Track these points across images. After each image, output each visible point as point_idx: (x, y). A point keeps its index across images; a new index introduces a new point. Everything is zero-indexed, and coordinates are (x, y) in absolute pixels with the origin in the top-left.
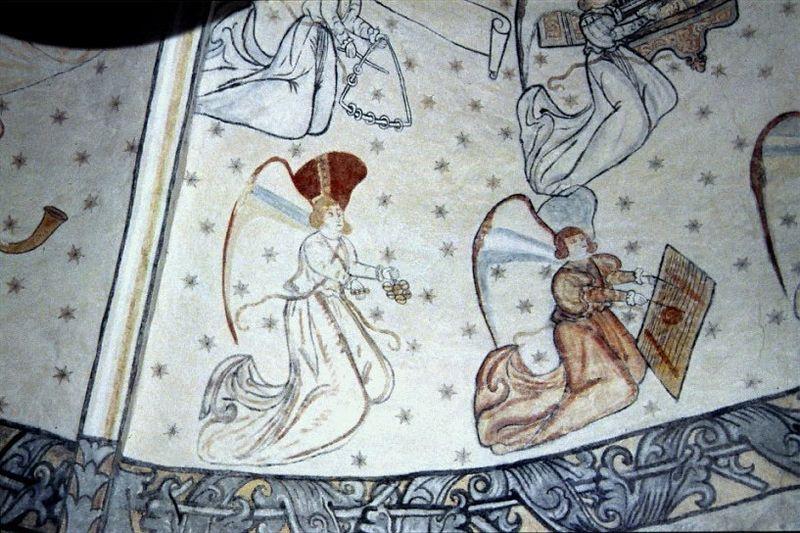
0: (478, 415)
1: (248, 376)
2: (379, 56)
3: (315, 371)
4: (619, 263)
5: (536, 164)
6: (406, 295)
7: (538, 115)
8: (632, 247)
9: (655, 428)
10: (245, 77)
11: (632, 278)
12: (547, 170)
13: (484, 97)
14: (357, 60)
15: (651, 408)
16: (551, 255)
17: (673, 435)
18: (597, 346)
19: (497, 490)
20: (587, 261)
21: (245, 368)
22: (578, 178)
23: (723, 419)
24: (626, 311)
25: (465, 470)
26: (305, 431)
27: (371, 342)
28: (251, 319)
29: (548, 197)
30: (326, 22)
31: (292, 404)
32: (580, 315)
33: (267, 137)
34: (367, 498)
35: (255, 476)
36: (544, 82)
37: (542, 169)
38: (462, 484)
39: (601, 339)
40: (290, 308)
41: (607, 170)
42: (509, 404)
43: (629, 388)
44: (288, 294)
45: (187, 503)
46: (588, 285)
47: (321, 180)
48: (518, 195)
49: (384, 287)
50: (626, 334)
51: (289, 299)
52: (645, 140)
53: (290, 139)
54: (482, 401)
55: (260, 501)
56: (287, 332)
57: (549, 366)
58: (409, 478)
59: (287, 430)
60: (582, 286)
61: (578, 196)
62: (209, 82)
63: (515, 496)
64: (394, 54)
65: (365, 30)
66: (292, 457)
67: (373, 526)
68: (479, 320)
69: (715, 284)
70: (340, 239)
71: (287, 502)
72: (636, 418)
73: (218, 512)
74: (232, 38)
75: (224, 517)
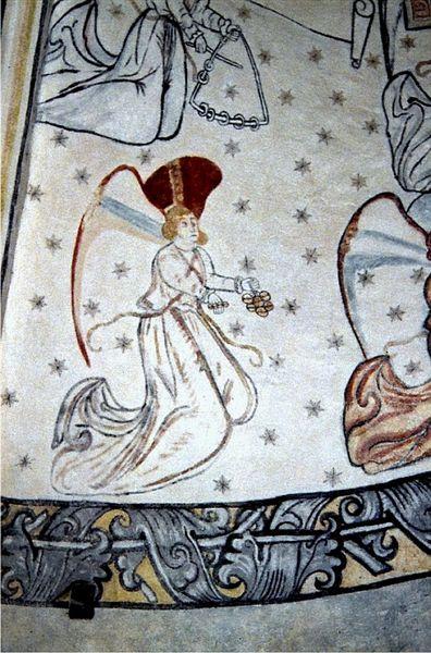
0: (347, 433)
1: (102, 400)
2: (233, 49)
3: (174, 394)
6: (268, 307)
7: (405, 104)
10: (87, 80)
12: (416, 166)
13: (347, 87)
14: (208, 55)
19: (370, 512)
21: (99, 390)
26: (164, 456)
27: (231, 358)
28: (103, 338)
29: (419, 194)
30: (172, 15)
31: (150, 429)
33: (114, 144)
34: (231, 525)
35: (113, 506)
36: (412, 68)
37: (411, 164)
38: (333, 507)
42: (381, 419)
44: (141, 311)
45: (40, 538)
47: (173, 187)
49: (243, 299)
51: (143, 317)
53: (139, 145)
54: (351, 418)
55: (119, 532)
56: (142, 351)
58: (277, 502)
59: (145, 456)
62: (48, 89)
63: (390, 517)
64: (247, 47)
65: (216, 20)
66: (151, 485)
67: (239, 555)
68: (344, 330)
70: (194, 250)
71: (147, 532)
73: (74, 546)
74: (73, 38)
75: (82, 551)
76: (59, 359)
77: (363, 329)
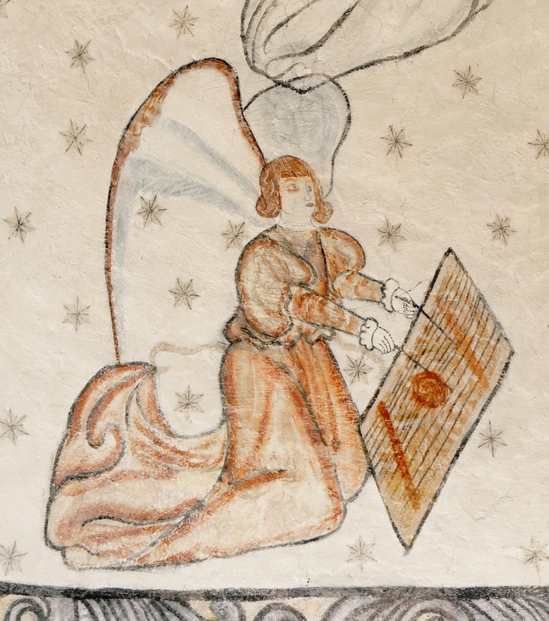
0: (56, 485)
4: (362, 263)
5: (263, 9)
8: (390, 234)
9: (361, 591)
11: (378, 296)
12: (280, 25)
15: (359, 551)
16: (249, 203)
17: (386, 612)
18: (292, 408)
20: (309, 237)
22: (329, 60)
23: (474, 606)
24: (356, 355)
25: (8, 585)
32: (274, 338)
39: (300, 397)
41: (380, 61)
42: (116, 478)
43: (329, 502)
46: (302, 285)
48: (213, 59)
50: (345, 400)
52: (462, 26)
57: (199, 424)
60: (289, 283)
61: (321, 98)
69: (512, 353)
72: (326, 565)
77: (126, 305)
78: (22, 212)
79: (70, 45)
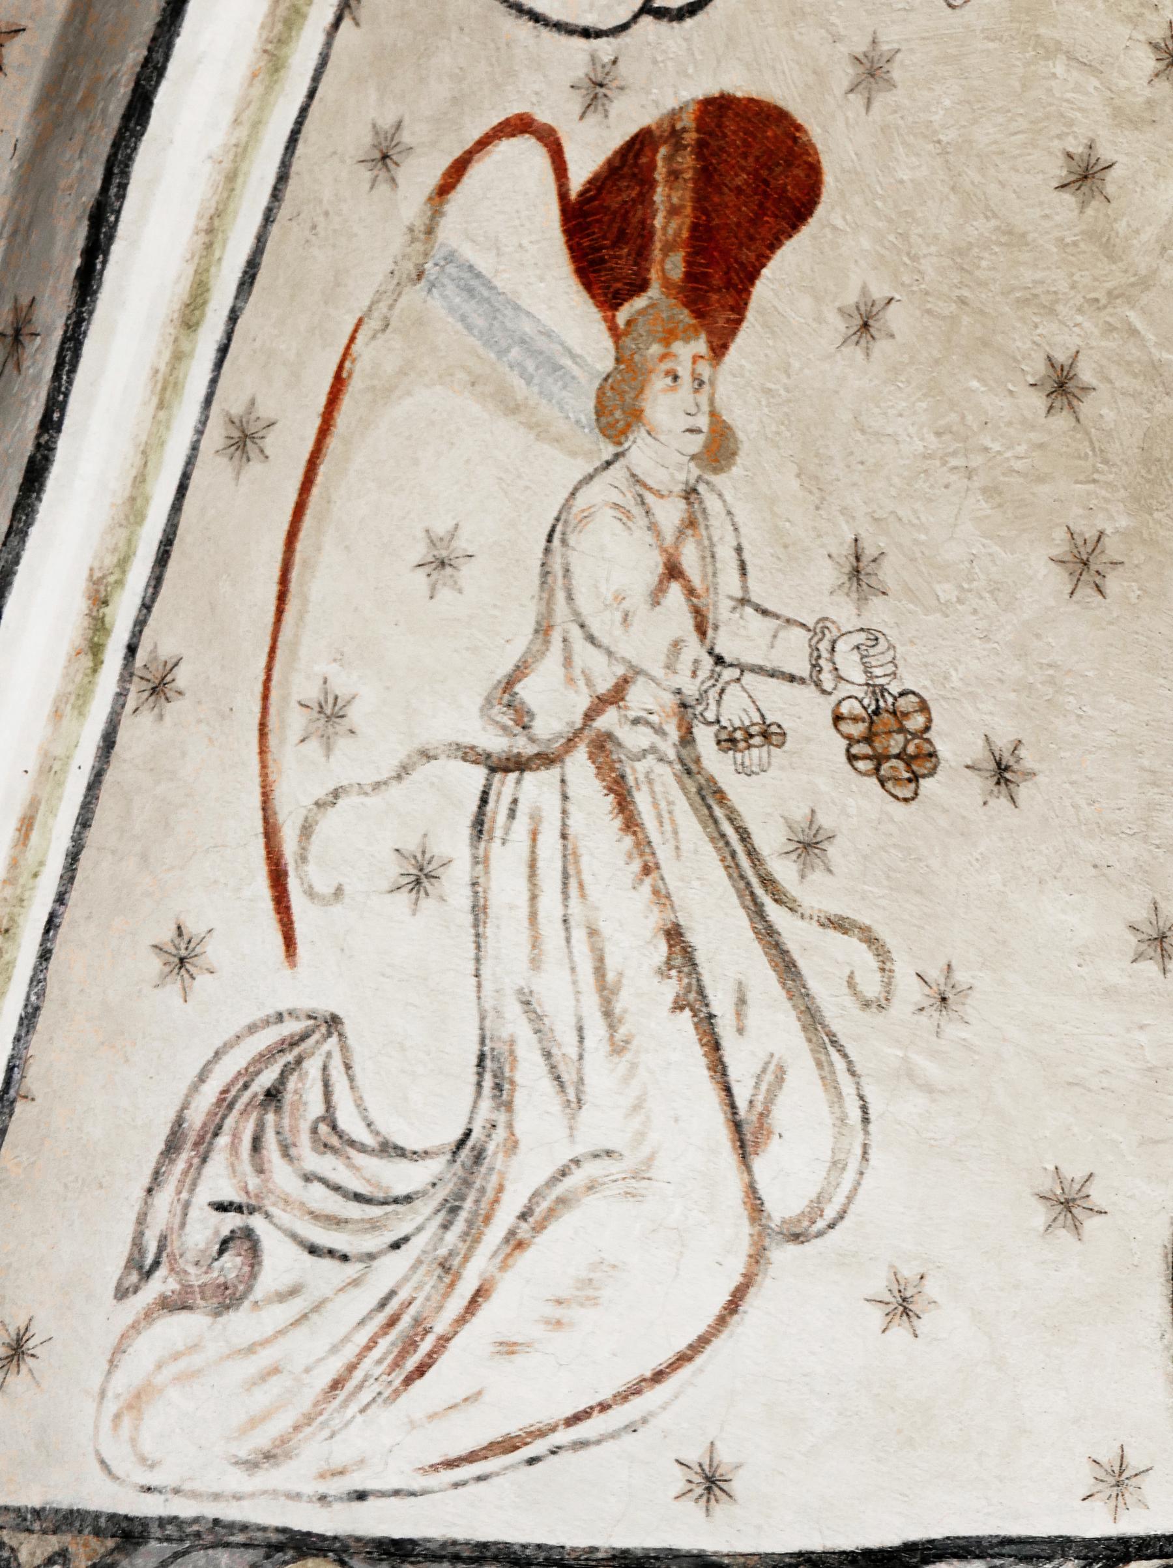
1: (316, 1108)
3: (571, 1092)
21: (312, 1067)
25: (1123, 1541)
26: (508, 1348)
27: (787, 967)
28: (347, 854)
31: (472, 1237)
40: (498, 810)
44: (496, 743)
47: (658, 222)
49: (838, 719)
56: (479, 911)
59: (444, 1341)
66: (451, 1464)
70: (690, 493)
76: (193, 928)
78: (1003, 743)
79: (1037, 368)
